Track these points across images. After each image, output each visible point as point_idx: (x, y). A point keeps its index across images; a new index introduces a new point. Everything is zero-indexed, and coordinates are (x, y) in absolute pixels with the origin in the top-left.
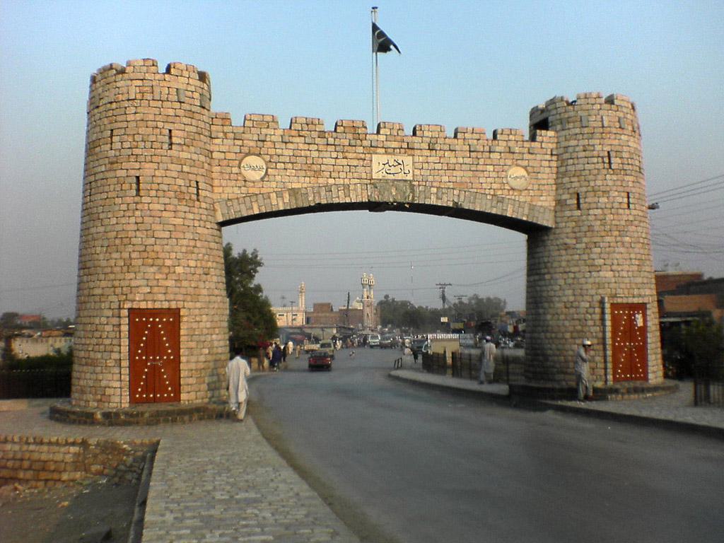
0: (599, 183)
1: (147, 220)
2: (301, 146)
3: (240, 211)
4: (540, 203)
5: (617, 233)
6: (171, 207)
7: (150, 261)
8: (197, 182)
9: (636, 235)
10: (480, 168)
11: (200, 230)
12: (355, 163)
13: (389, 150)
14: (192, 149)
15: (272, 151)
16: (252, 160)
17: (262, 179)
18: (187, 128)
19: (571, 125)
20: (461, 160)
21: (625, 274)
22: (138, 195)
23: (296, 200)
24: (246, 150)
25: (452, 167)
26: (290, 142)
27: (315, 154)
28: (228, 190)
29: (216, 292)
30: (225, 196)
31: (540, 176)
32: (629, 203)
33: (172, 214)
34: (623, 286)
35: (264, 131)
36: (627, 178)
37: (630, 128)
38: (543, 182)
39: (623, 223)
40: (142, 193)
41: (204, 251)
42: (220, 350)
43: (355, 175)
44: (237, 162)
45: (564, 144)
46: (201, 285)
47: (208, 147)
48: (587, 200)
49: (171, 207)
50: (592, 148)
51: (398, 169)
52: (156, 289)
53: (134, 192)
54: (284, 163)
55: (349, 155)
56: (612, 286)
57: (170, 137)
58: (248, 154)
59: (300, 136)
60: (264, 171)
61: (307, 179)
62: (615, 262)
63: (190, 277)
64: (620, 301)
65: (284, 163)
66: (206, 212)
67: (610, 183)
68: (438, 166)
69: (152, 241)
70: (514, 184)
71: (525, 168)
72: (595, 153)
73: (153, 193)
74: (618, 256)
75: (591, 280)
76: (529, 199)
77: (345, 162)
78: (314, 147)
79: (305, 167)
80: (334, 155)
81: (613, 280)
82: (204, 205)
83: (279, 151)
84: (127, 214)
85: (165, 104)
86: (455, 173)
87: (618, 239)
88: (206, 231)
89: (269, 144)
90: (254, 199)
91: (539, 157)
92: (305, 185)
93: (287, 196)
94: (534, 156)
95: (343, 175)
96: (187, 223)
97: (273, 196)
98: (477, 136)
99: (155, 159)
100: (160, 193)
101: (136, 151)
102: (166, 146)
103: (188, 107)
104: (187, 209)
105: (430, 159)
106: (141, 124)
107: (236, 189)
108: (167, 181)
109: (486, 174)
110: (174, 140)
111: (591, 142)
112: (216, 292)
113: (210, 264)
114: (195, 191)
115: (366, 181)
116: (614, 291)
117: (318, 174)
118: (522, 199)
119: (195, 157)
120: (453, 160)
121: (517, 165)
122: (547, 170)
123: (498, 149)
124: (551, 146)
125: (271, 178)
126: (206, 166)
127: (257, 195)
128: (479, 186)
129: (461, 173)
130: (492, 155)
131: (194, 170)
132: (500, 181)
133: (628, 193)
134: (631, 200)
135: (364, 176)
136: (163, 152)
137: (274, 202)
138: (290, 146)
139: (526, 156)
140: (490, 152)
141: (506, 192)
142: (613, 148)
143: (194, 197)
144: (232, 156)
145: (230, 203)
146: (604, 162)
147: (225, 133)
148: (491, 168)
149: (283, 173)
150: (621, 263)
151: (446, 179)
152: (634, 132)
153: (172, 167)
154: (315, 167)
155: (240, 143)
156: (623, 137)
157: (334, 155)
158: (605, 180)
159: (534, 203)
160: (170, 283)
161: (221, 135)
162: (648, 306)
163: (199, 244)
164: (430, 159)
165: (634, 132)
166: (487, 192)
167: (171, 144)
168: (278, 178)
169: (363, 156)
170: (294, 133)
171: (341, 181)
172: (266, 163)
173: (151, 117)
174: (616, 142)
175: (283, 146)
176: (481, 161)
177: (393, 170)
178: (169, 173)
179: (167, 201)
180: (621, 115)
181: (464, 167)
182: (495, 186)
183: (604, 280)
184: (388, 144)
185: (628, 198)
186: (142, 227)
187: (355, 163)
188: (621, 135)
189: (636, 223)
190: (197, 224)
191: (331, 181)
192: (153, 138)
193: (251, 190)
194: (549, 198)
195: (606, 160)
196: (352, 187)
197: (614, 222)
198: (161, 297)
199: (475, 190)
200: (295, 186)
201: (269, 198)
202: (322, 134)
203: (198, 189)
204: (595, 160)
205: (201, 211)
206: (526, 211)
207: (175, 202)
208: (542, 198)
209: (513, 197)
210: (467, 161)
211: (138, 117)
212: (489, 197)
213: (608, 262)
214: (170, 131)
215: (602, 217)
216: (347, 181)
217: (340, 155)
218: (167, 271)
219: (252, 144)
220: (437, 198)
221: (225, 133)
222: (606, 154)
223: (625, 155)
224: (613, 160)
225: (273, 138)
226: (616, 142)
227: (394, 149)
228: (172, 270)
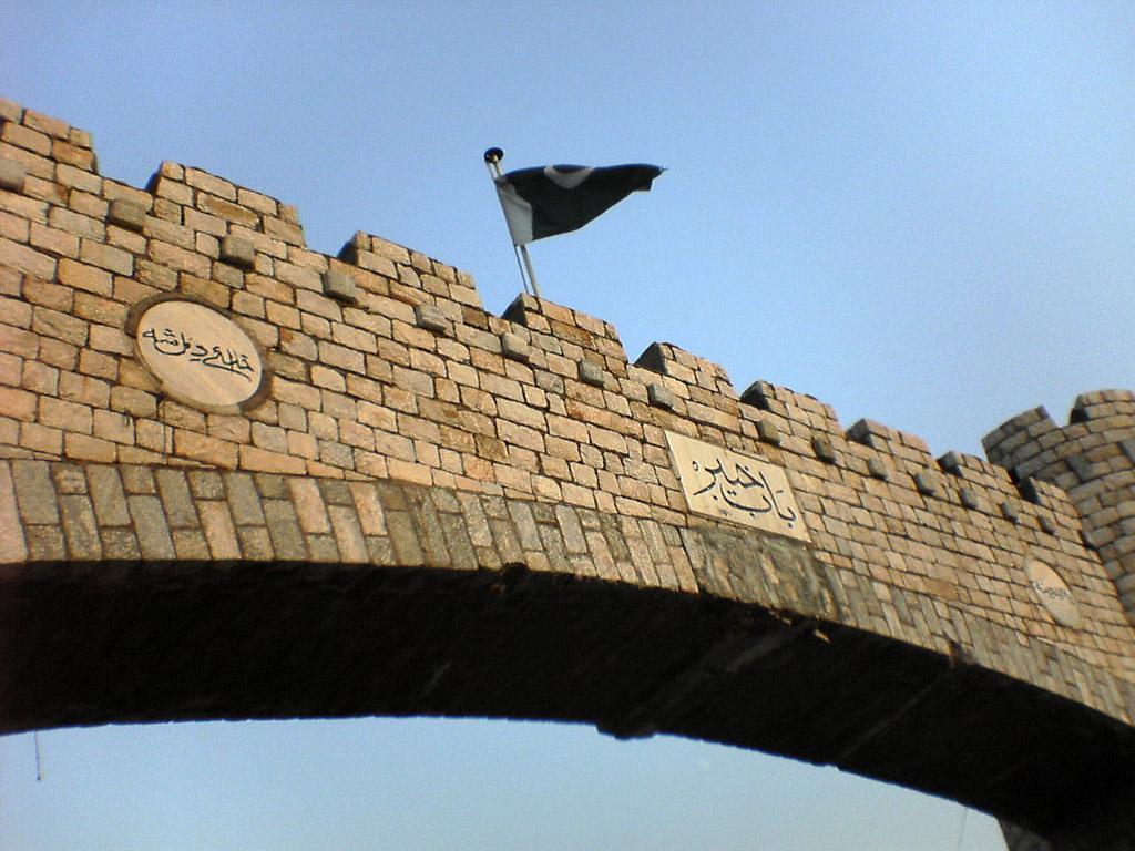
3: (130, 527)
17: (247, 408)
19: (1100, 468)
28: (57, 413)
30: (43, 439)
44: (122, 311)
45: (1111, 514)
54: (344, 372)
55: (590, 413)
60: (257, 378)
61: (451, 458)
65: (344, 372)
92: (446, 480)
93: (376, 507)
107: (111, 425)
127: (221, 470)
135: (658, 495)
145: (71, 478)
149: (338, 404)
168: (322, 423)
172: (264, 352)
193: (192, 445)
201: (287, 496)
202: (476, 317)
217: (558, 405)
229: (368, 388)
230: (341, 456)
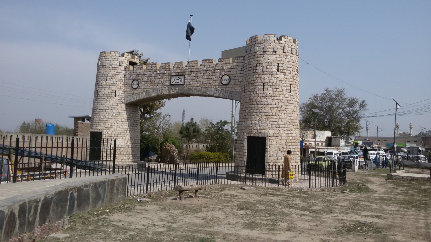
4: (234, 91)
6: (105, 100)
8: (115, 91)
9: (266, 103)
11: (114, 106)
14: (114, 80)
29: (121, 127)
31: (235, 78)
32: (264, 88)
36: (263, 76)
37: (272, 50)
38: (237, 81)
42: (121, 146)
49: (105, 100)
63: (109, 122)
64: (252, 135)
66: (119, 100)
76: (230, 89)
82: (118, 98)
88: (118, 107)
96: (110, 104)
107: (131, 92)
110: (108, 78)
112: (121, 127)
114: (114, 94)
118: (227, 89)
122: (239, 75)
124: (241, 64)
133: (264, 83)
134: (265, 87)
143: (114, 96)
162: (267, 138)
163: (114, 111)
165: (276, 52)
185: (264, 85)
194: (239, 88)
195: (255, 68)
196: (164, 89)
200: (147, 89)
203: (115, 93)
204: (250, 69)
205: (116, 100)
206: (228, 94)
208: (236, 88)
209: (223, 89)
212: (213, 89)
230: (143, 90)
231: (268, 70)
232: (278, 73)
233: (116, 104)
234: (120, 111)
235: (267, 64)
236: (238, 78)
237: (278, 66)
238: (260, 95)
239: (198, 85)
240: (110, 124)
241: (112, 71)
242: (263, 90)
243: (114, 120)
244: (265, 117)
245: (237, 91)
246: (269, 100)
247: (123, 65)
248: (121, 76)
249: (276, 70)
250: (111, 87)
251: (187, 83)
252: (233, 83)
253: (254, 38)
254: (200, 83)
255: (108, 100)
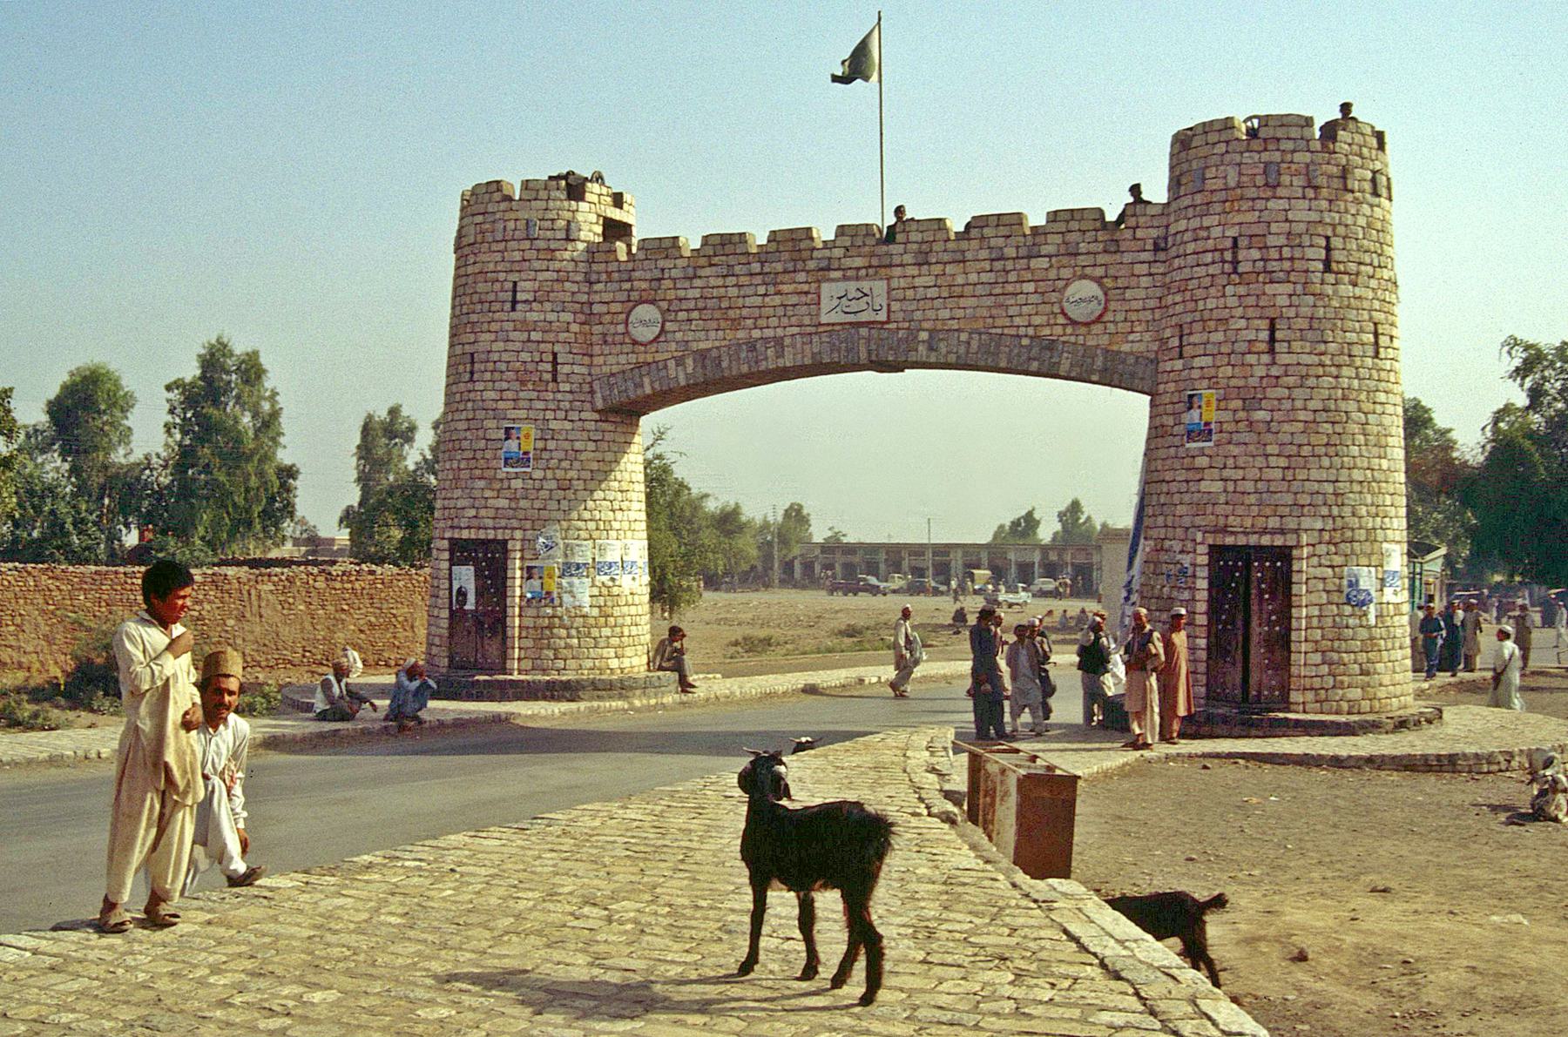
0: (1211, 304)
1: (480, 414)
2: (713, 282)
4: (1126, 348)
5: (1240, 403)
6: (510, 395)
7: (478, 472)
8: (555, 355)
9: (1287, 405)
10: (1010, 288)
11: (553, 425)
12: (794, 299)
13: (849, 273)
14: (548, 306)
15: (671, 294)
16: (645, 312)
17: (655, 340)
18: (541, 276)
20: (973, 278)
21: (1249, 486)
22: (471, 380)
23: (704, 367)
24: (635, 295)
25: (958, 290)
26: (695, 277)
27: (733, 292)
30: (606, 369)
31: (1129, 294)
32: (1272, 340)
33: (511, 404)
34: (1240, 510)
35: (661, 264)
36: (1269, 289)
37: (1299, 181)
39: (1253, 382)
40: (476, 376)
41: (561, 455)
43: (793, 320)
46: (553, 505)
47: (584, 298)
48: (1193, 339)
49: (510, 395)
50: (1205, 234)
51: (862, 304)
52: (483, 512)
53: (467, 376)
55: (785, 288)
56: (1219, 510)
57: (515, 291)
58: (641, 302)
59: (711, 265)
62: (1230, 462)
66: (569, 397)
67: (1232, 302)
68: (932, 293)
69: (482, 444)
70: (1075, 313)
71: (1098, 281)
72: (1210, 244)
73: (488, 376)
74: (1235, 450)
75: (1187, 498)
76: (1104, 340)
77: (777, 300)
78: (731, 281)
79: (717, 314)
80: (761, 290)
81: (1222, 499)
82: (567, 387)
83: (681, 293)
84: (462, 407)
85: (512, 244)
86: (963, 303)
87: (1242, 415)
88: (568, 425)
89: (667, 283)
90: (644, 370)
91: (1127, 258)
94: (1117, 257)
95: (774, 322)
97: (672, 364)
98: (1003, 231)
99: (494, 326)
100: (497, 376)
101: (474, 318)
102: (508, 306)
103: (541, 244)
104: (534, 395)
105: (917, 281)
106: (480, 278)
107: (623, 359)
108: (505, 357)
109: (1021, 299)
110: (520, 296)
111: (1207, 222)
113: (572, 474)
114: (549, 367)
115: (809, 329)
116: (1222, 521)
117: (736, 324)
119: (552, 317)
120: (960, 280)
121: (1084, 277)
122: (1145, 281)
123: (1045, 250)
124: (1154, 233)
125: (669, 336)
126: (575, 328)
128: (1007, 322)
129: (971, 302)
130: (1034, 263)
131: (551, 337)
132: (1047, 308)
133: (1272, 320)
134: (1279, 335)
135: (807, 321)
136: (503, 316)
137: (672, 373)
138: (697, 283)
139: (1101, 259)
140: (1029, 257)
141: (1058, 330)
142: (1245, 230)
143: (548, 377)
144: (616, 307)
146: (1224, 261)
147: (609, 273)
148: (1030, 287)
150: (1240, 462)
151: (945, 314)
152: (1316, 188)
153: (513, 335)
154: (731, 313)
155: (627, 286)
156: (1271, 204)
157: (761, 290)
158: (1224, 296)
159: (1115, 348)
160: (503, 503)
161: (604, 277)
162: (1295, 553)
164: (917, 281)
165: (1316, 188)
166: (1022, 331)
167: (514, 302)
168: (679, 336)
169: (805, 287)
170: (703, 261)
171: (769, 333)
172: (663, 313)
173: (491, 267)
174: (1252, 217)
175: (687, 284)
176: (1012, 277)
177: (854, 306)
178: (510, 346)
179: (505, 385)
180: (1277, 156)
181: (980, 290)
182: (1037, 320)
183: (1206, 498)
184: (847, 262)
186: (473, 424)
187: (794, 299)
188: (1268, 199)
189: (1291, 380)
190: (550, 415)
191: (756, 334)
192: (492, 297)
194: (1147, 337)
195: (1228, 256)
196: (787, 341)
197: (1233, 382)
198: (490, 523)
199: (999, 331)
200: (702, 346)
201: (666, 367)
203: (555, 363)
204: (1208, 258)
205: (559, 396)
207: (517, 385)
208: (1131, 337)
209: (1073, 339)
210: (985, 277)
211: (477, 268)
213: (1219, 462)
214: (515, 283)
215: (1212, 372)
216: (780, 332)
217: (771, 289)
218: (497, 485)
219: (644, 285)
220: (931, 349)
221: (609, 273)
222: (1229, 243)
223: (1271, 240)
224: (1241, 255)
225: (674, 273)
226: (1252, 217)
227: (858, 269)
228: (506, 484)
229: (695, 315)
231: (1287, 265)
232: (1330, 278)
233: (561, 414)
234: (578, 445)
235: (1282, 240)
236: (1142, 294)
237: (1328, 249)
238: (1260, 371)
239: (954, 324)
240: (537, 504)
241: (537, 265)
242: (1272, 351)
243: (553, 485)
244: (1283, 462)
245: (1137, 347)
246: (1297, 393)
247: (583, 235)
248: (575, 288)
249: (1320, 266)
250: (535, 336)
251: (900, 316)
252: (1120, 317)
253: (1217, 127)
254: (960, 313)
255: (522, 395)
